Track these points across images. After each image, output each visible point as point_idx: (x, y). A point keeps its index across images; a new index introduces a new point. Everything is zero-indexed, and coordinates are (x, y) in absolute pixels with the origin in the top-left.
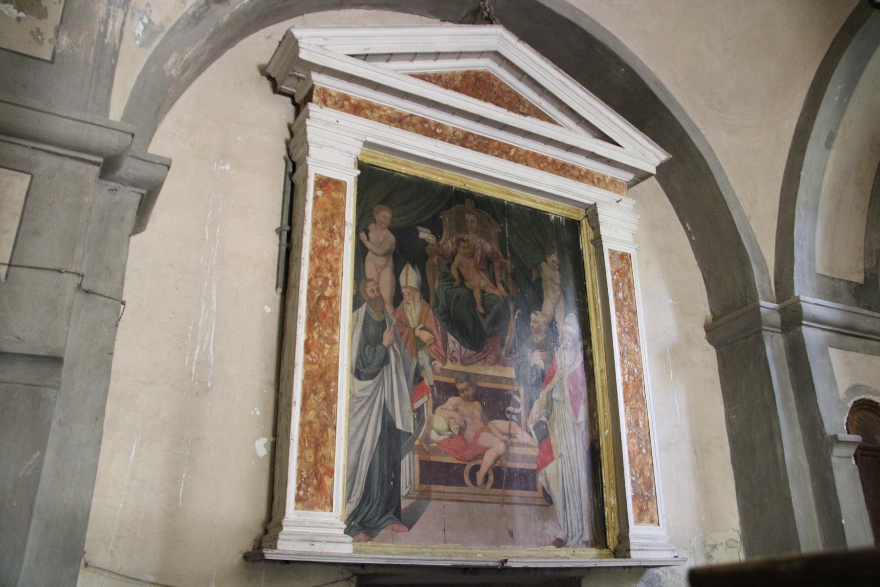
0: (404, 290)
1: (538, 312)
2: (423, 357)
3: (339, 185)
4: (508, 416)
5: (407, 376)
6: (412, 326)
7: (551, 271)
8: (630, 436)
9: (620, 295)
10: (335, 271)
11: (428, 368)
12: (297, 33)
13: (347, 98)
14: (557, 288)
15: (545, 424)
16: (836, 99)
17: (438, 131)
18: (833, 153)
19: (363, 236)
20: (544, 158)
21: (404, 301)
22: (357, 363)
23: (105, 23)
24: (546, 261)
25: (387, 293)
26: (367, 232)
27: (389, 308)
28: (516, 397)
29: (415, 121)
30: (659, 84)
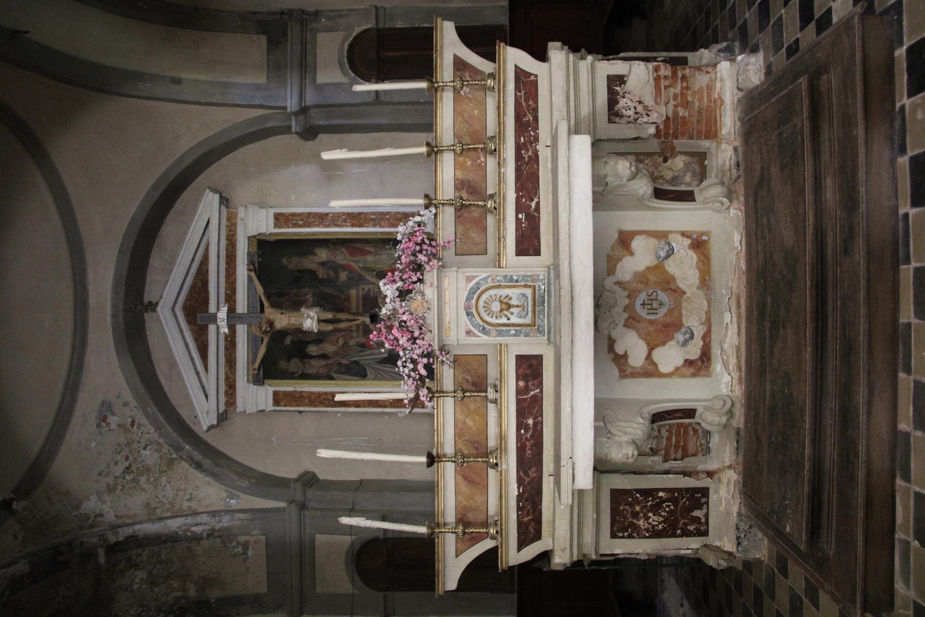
0: (320, 353)
2: (352, 342)
3: (276, 394)
5: (361, 351)
7: (293, 263)
8: (381, 226)
9: (300, 223)
10: (320, 394)
11: (357, 340)
12: (205, 428)
13: (226, 392)
16: (149, 85)
18: (184, 76)
19: (296, 375)
20: (227, 270)
23: (243, 520)
25: (324, 362)
26: (293, 373)
27: (330, 362)
30: (154, 187)
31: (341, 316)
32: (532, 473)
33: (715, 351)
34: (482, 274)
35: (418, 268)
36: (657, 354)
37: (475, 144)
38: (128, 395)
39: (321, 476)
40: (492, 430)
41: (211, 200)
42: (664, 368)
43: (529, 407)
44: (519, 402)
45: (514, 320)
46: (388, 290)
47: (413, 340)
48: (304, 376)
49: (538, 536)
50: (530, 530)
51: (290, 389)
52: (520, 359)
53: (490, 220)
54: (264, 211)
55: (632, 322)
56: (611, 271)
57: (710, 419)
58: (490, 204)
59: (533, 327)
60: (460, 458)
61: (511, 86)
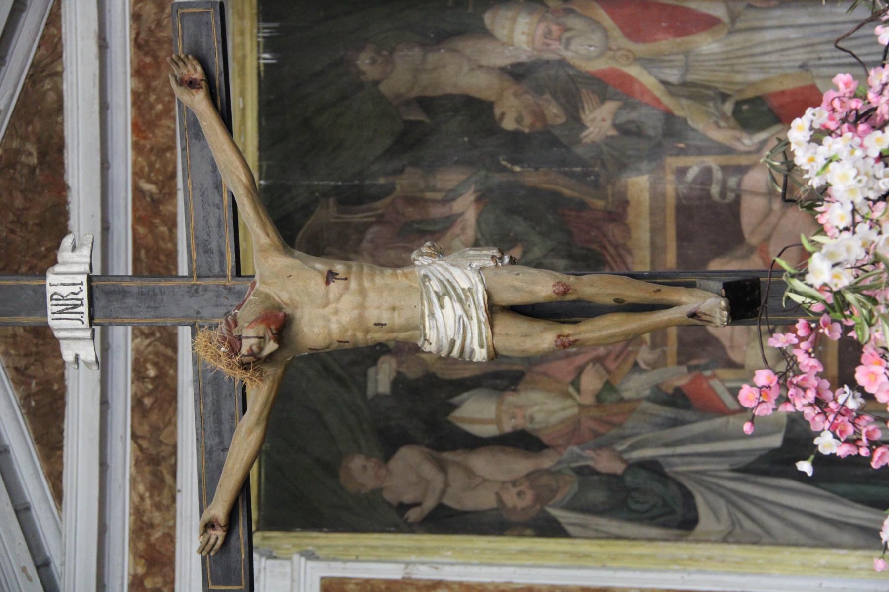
0: (508, 427)
1: (497, 112)
2: (635, 386)
4: (731, 196)
5: (675, 423)
6: (575, 410)
14: (433, 58)
15: (738, 104)
17: (152, 373)
19: (413, 515)
21: (529, 426)
22: (665, 526)
24: (376, 83)
26: (403, 508)
27: (547, 462)
28: (691, 175)
29: (146, 428)
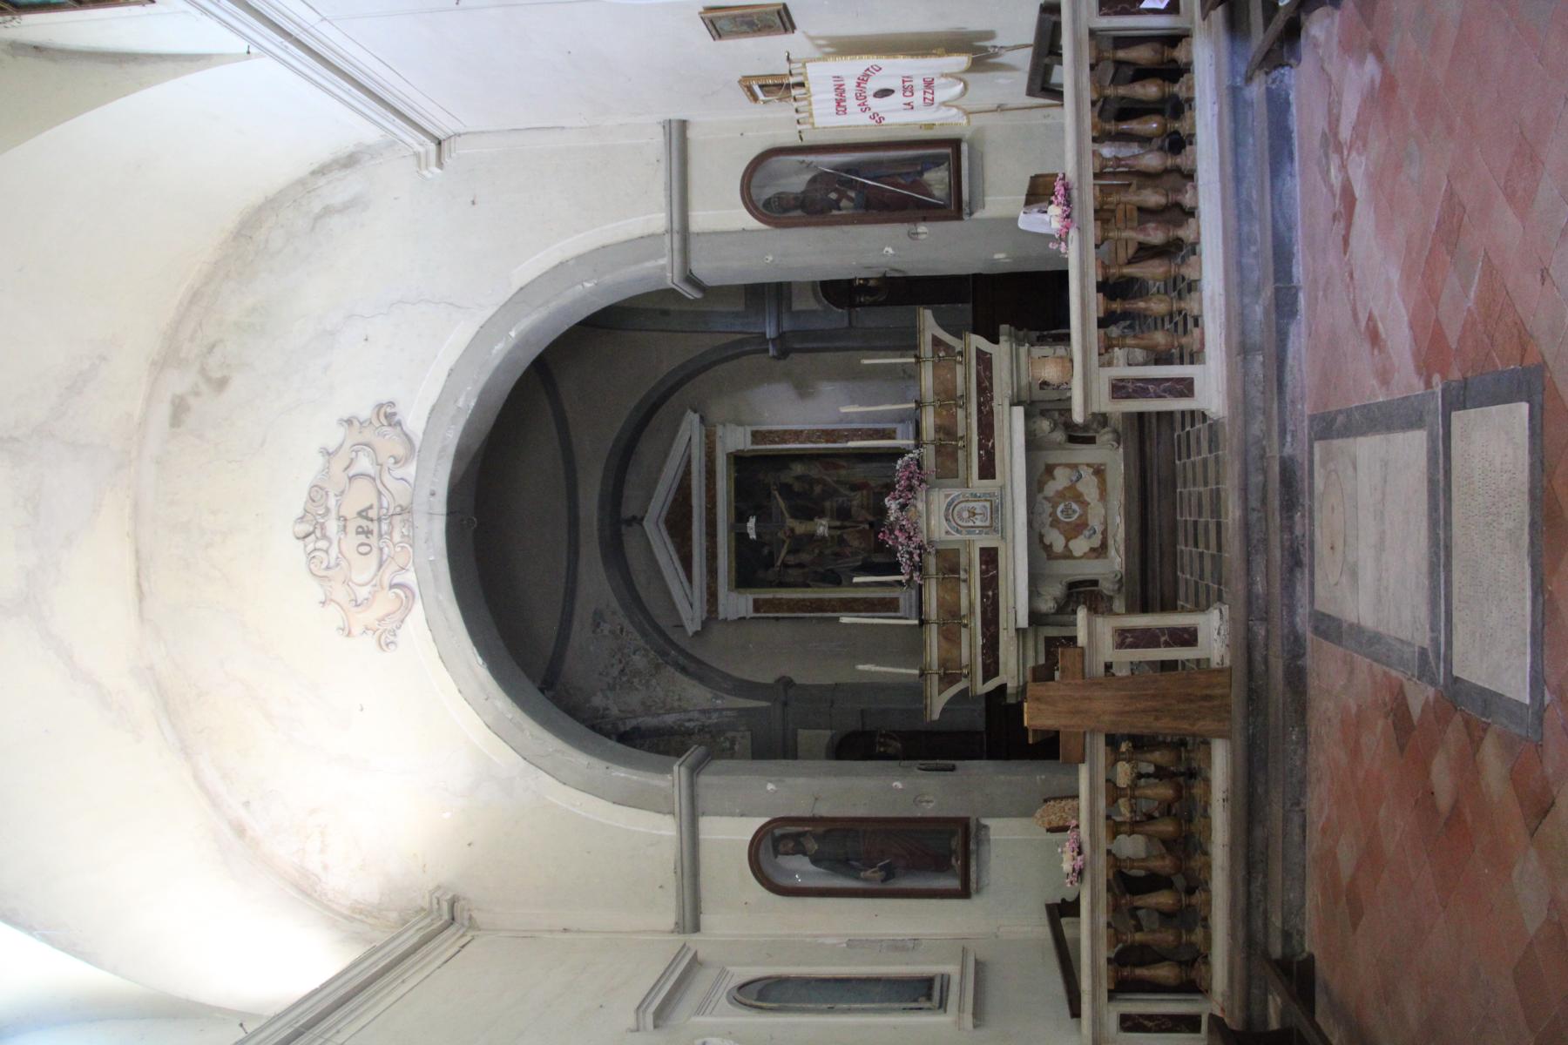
2: (827, 552)
3: (756, 601)
31: (847, 523)
32: (992, 629)
33: (1111, 542)
34: (955, 492)
35: (911, 488)
36: (1072, 544)
37: (948, 398)
38: (615, 604)
39: (798, 681)
40: (964, 603)
41: (692, 418)
42: (1077, 553)
43: (990, 583)
44: (982, 580)
45: (978, 523)
46: (892, 504)
47: (910, 538)
48: (782, 585)
49: (996, 674)
50: (991, 670)
51: (769, 596)
52: (982, 550)
53: (961, 454)
54: (741, 429)
55: (1055, 523)
56: (1041, 490)
57: (1107, 587)
58: (960, 444)
59: (991, 529)
60: (942, 625)
61: (974, 362)
